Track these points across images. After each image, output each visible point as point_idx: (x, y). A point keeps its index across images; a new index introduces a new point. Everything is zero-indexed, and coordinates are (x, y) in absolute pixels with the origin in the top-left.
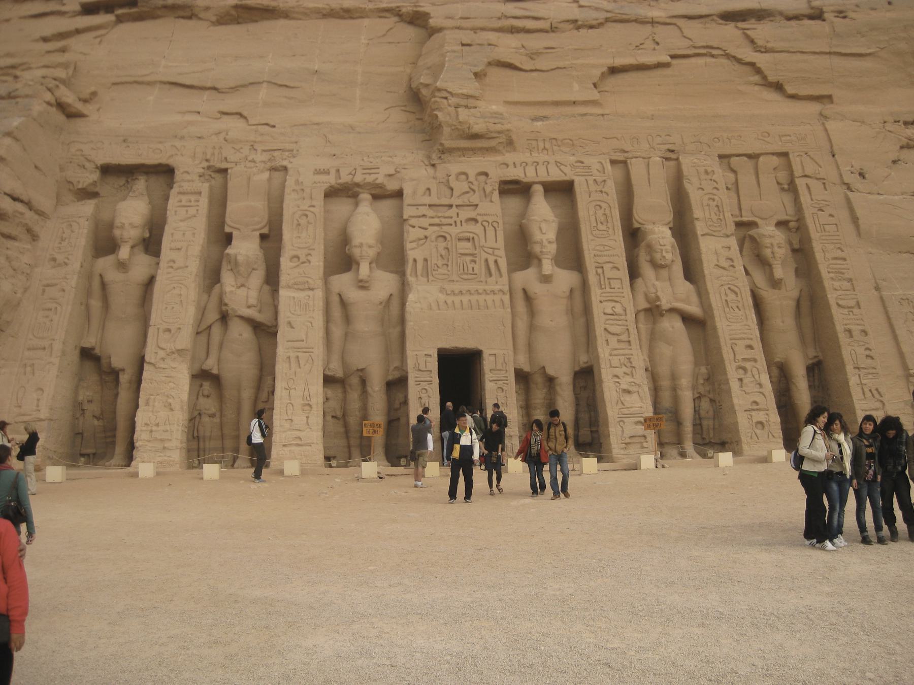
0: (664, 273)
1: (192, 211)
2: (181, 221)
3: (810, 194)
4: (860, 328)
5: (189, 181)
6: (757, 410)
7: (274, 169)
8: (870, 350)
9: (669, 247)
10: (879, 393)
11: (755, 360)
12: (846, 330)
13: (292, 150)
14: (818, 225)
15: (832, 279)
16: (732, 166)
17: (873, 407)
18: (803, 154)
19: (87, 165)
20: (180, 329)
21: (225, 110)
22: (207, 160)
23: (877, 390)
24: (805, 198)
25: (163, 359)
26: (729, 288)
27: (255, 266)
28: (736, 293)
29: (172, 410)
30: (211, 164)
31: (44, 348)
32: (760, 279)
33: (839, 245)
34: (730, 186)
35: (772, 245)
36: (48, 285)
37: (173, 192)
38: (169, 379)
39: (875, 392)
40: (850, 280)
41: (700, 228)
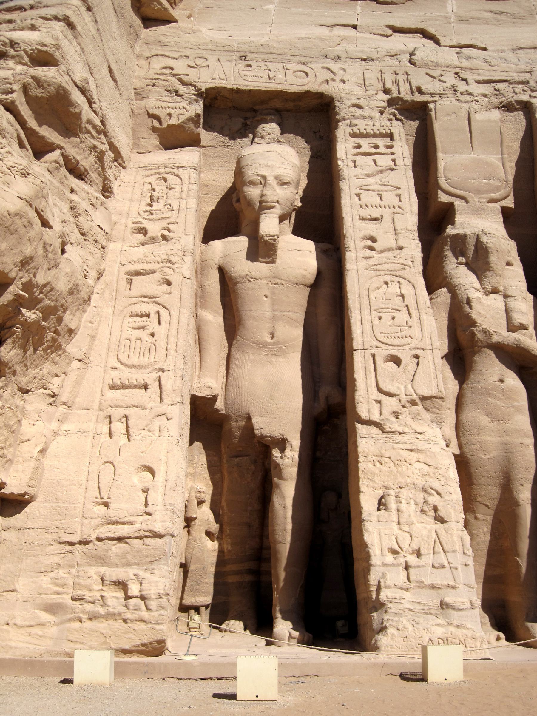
1: (384, 161)
2: (368, 176)
5: (364, 118)
7: (507, 107)
13: (528, 82)
19: (182, 89)
20: (417, 356)
21: (398, 24)
22: (386, 91)
25: (396, 415)
27: (509, 259)
29: (441, 520)
30: (395, 94)
31: (146, 387)
36: (137, 273)
37: (342, 132)
38: (414, 455)
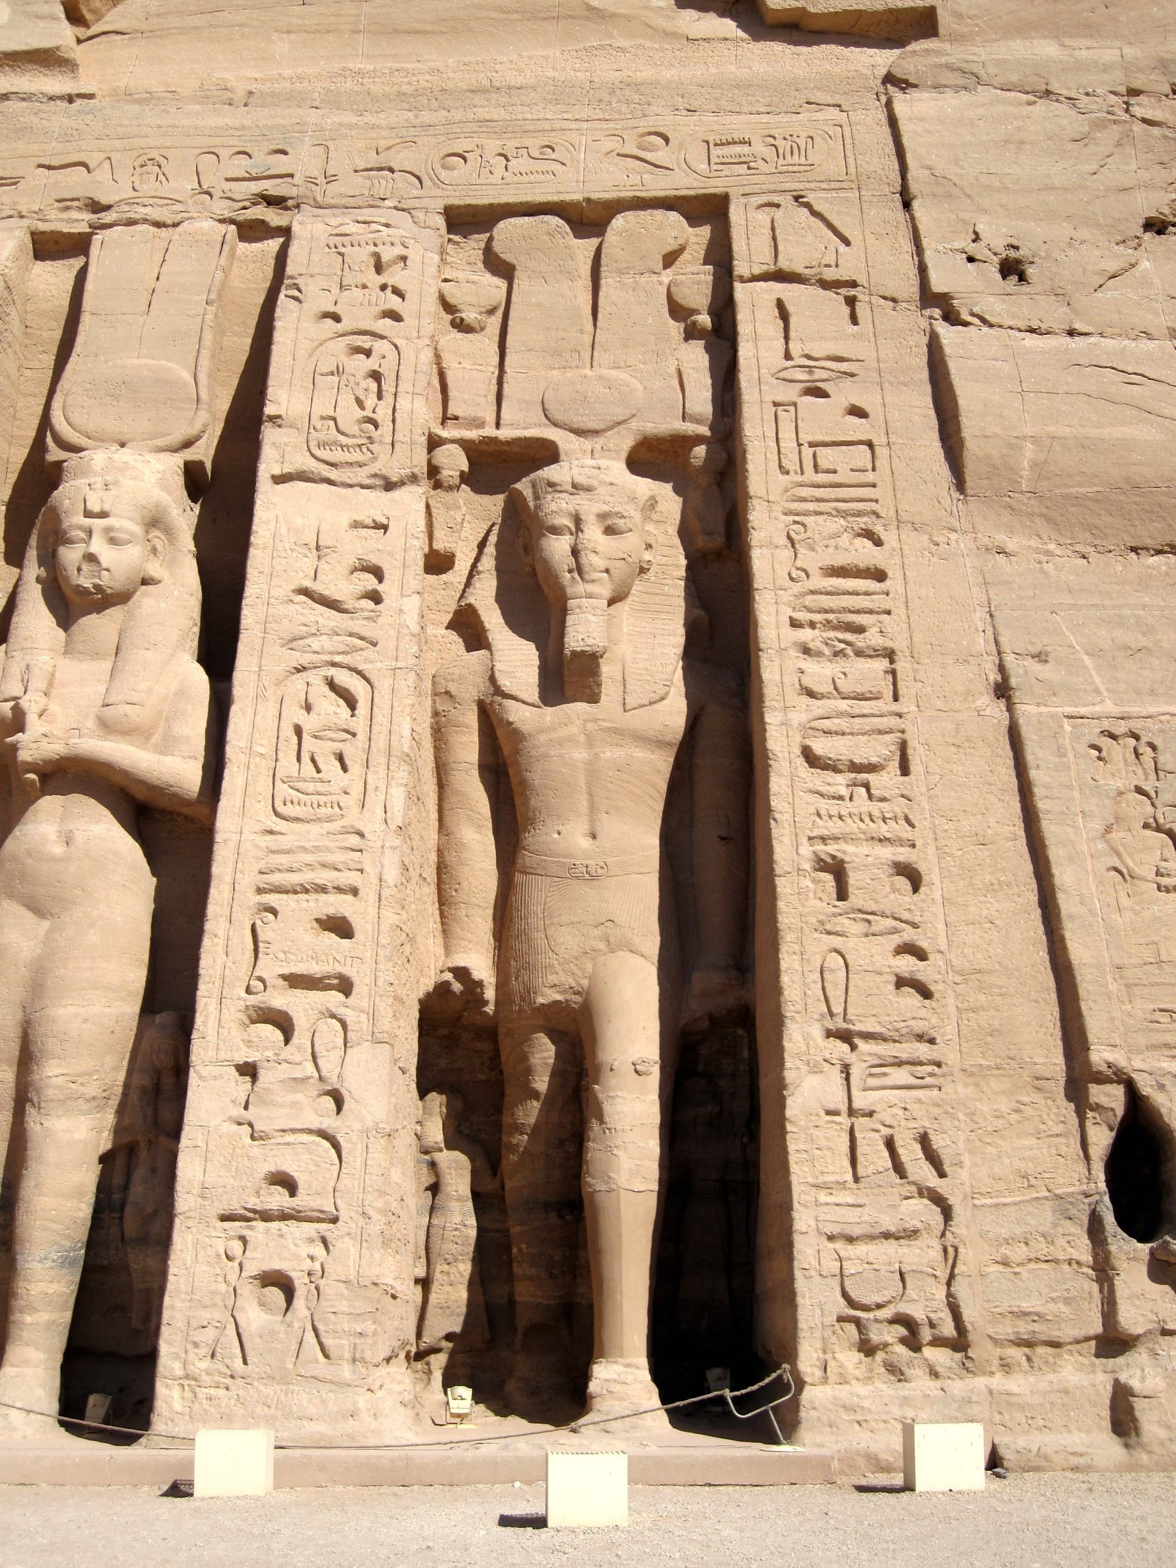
0: (99, 627)
3: (787, 338)
4: (887, 853)
6: (284, 1216)
8: (921, 955)
9: (126, 523)
10: (933, 1158)
11: (345, 986)
12: (822, 865)
14: (789, 443)
15: (806, 651)
16: (497, 247)
17: (888, 1223)
18: (786, 200)
23: (924, 1140)
24: (758, 347)
26: (332, 685)
28: (352, 704)
32: (517, 660)
33: (863, 522)
34: (470, 316)
35: (578, 520)
39: (911, 1153)
40: (890, 655)
41: (277, 451)
